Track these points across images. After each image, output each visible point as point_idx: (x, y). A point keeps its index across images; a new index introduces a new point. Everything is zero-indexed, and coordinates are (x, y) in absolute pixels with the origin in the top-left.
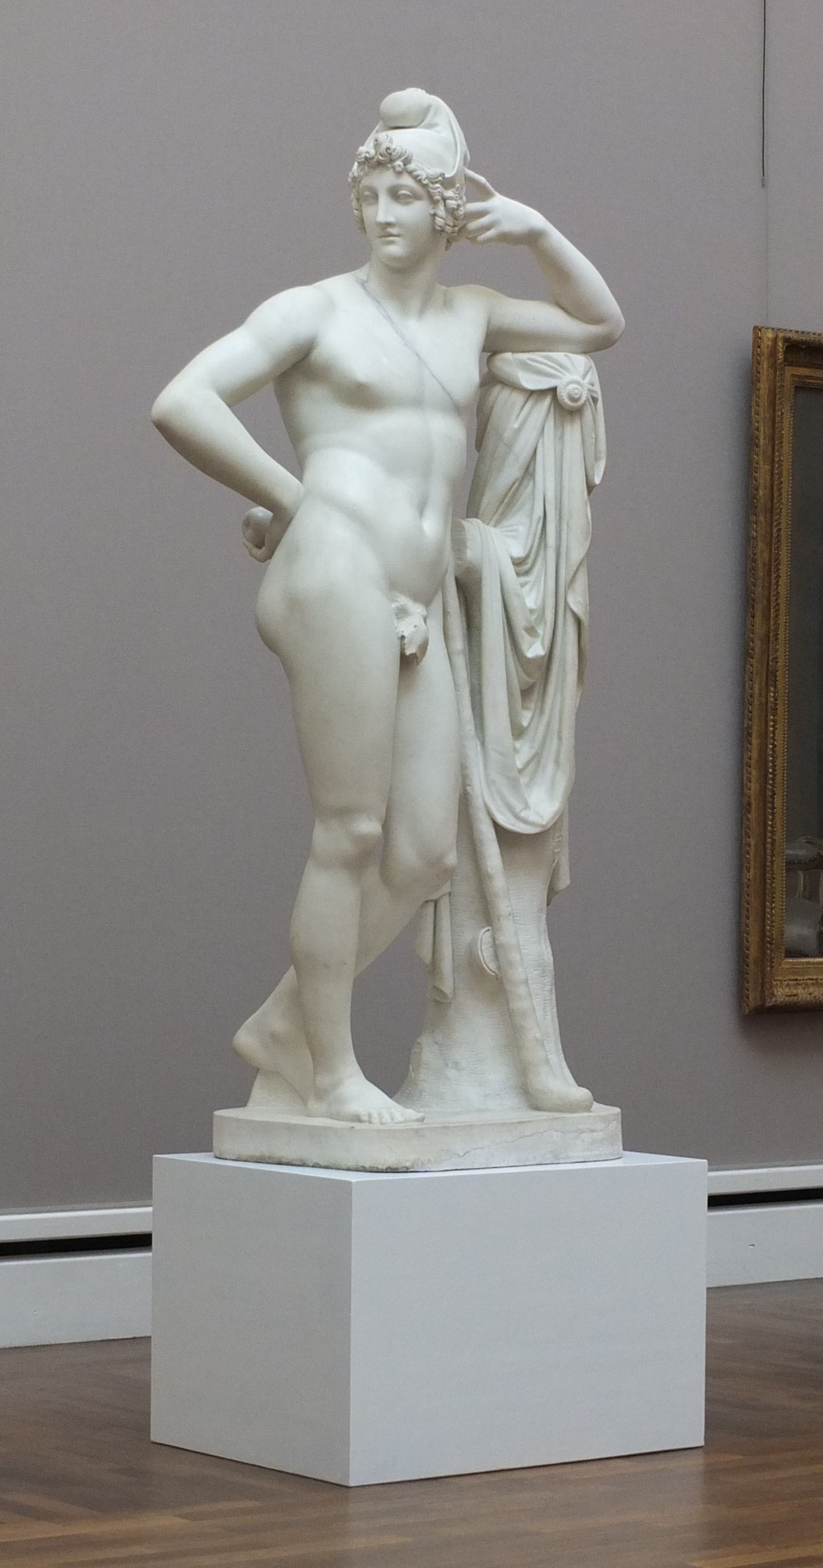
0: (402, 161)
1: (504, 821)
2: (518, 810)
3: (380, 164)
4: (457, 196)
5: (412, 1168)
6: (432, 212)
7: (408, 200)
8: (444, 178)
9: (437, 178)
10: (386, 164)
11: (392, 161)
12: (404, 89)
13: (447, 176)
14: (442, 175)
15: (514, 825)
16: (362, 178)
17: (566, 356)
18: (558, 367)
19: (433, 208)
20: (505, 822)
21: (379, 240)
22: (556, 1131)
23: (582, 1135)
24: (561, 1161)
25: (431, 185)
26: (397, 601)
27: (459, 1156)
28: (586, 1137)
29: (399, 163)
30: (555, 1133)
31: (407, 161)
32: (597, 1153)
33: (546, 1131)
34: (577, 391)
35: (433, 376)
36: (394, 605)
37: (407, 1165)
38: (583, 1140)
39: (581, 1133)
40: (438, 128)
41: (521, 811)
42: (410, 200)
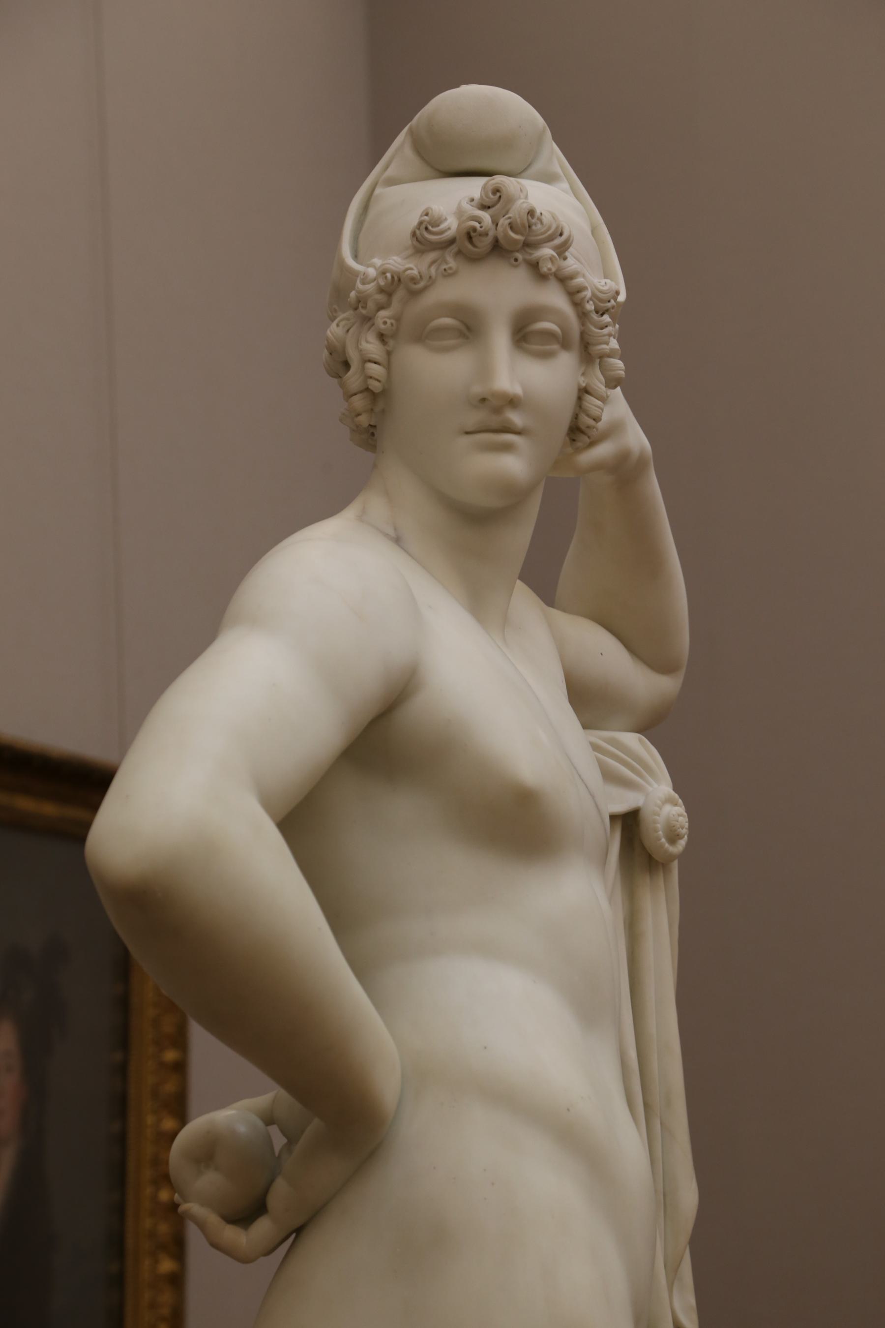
0: (555, 248)
3: (498, 249)
6: (583, 381)
7: (547, 347)
10: (512, 252)
11: (528, 245)
12: (458, 86)
16: (431, 282)
18: (629, 759)
19: (583, 374)
21: (466, 441)
25: (595, 316)
29: (546, 251)
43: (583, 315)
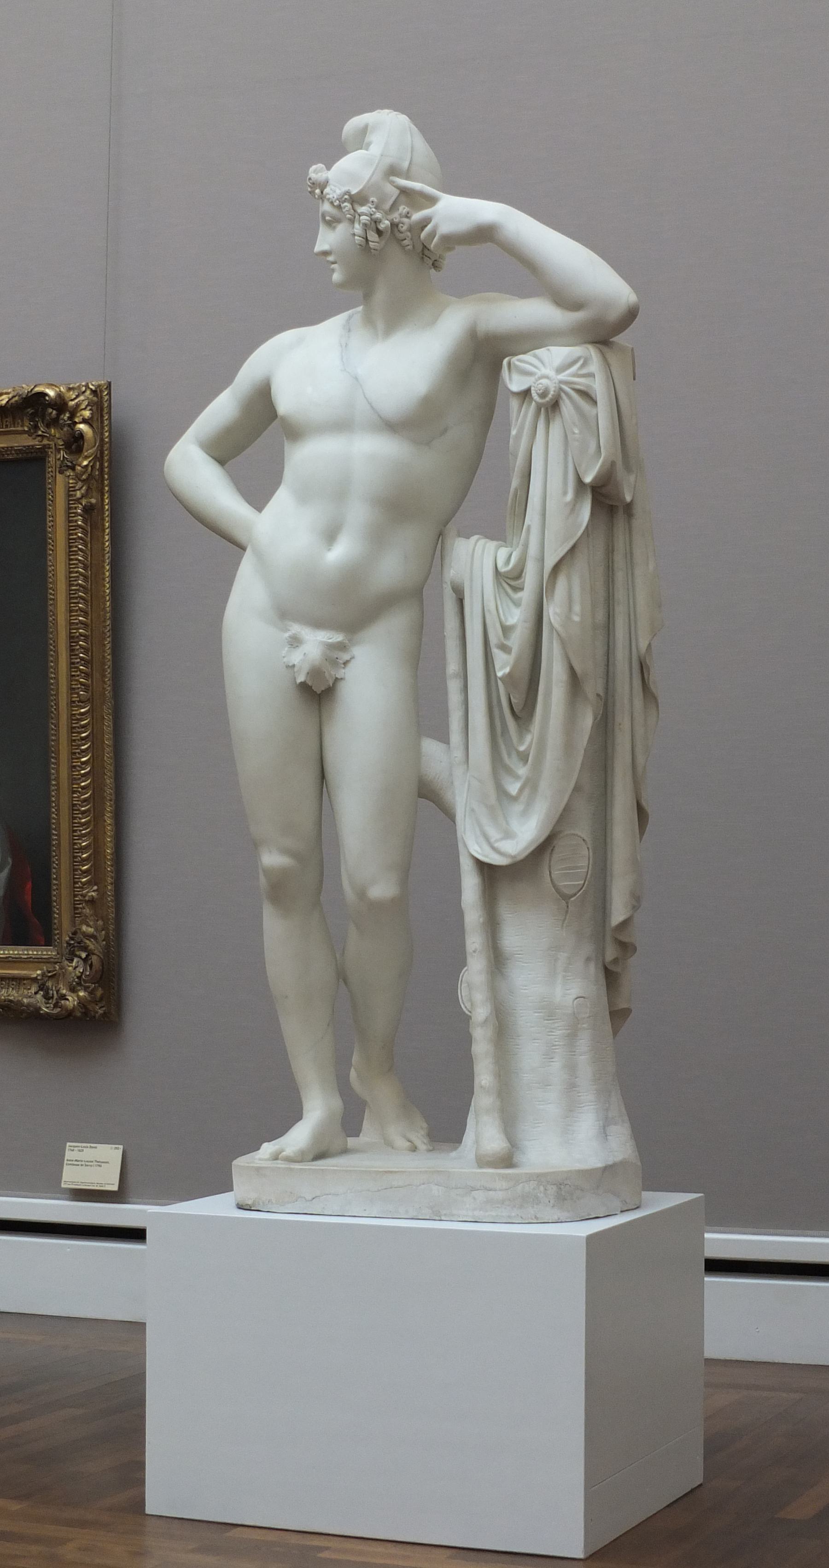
1: (477, 852)
2: (492, 840)
4: (374, 210)
5: (253, 1207)
8: (350, 196)
9: (343, 196)
13: (354, 191)
14: (348, 193)
15: (486, 856)
17: (548, 350)
20: (477, 852)
22: (436, 1185)
23: (473, 1192)
24: (443, 1218)
26: (289, 630)
27: (305, 1199)
28: (480, 1195)
29: (318, 191)
30: (435, 1188)
31: (323, 185)
32: (494, 1214)
33: (423, 1184)
34: (541, 385)
35: (365, 396)
36: (287, 635)
37: (249, 1203)
38: (474, 1198)
39: (471, 1191)
40: (372, 147)
41: (497, 841)
42: (334, 224)
43: (339, 207)
